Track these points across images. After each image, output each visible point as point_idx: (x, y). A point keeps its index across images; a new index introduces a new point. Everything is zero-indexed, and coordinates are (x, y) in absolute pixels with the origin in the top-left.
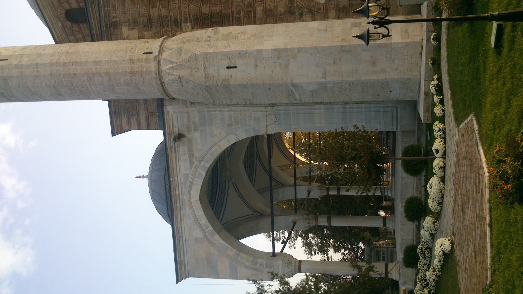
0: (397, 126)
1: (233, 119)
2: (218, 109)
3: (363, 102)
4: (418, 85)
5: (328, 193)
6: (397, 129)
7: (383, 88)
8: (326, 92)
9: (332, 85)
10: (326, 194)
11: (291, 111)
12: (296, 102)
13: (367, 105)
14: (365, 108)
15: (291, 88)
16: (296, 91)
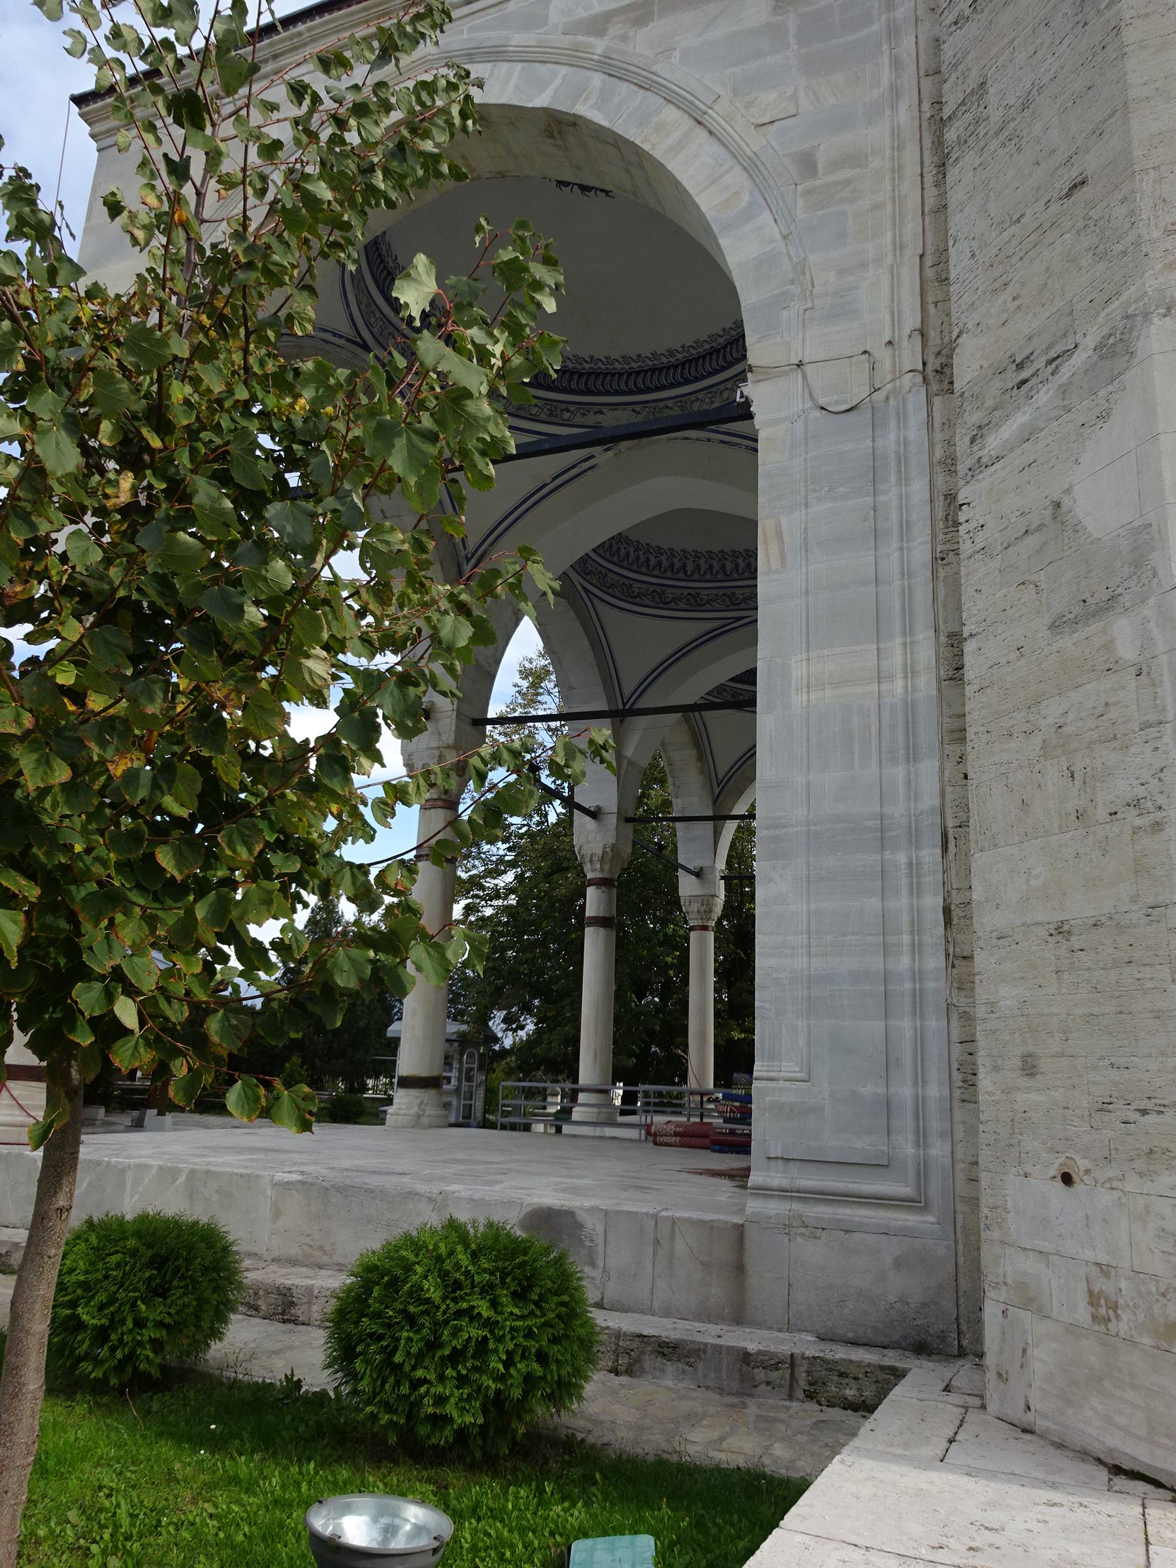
0: (784, 1193)
1: (841, 175)
2: (910, 72)
3: (959, 960)
4: (1141, 1454)
5: (591, 883)
6: (763, 1191)
7: (1105, 1107)
8: (1056, 626)
9: (1127, 651)
10: (590, 876)
11: (894, 493)
12: (962, 444)
13: (936, 986)
14: (917, 976)
15: (1090, 342)
16: (1064, 390)
